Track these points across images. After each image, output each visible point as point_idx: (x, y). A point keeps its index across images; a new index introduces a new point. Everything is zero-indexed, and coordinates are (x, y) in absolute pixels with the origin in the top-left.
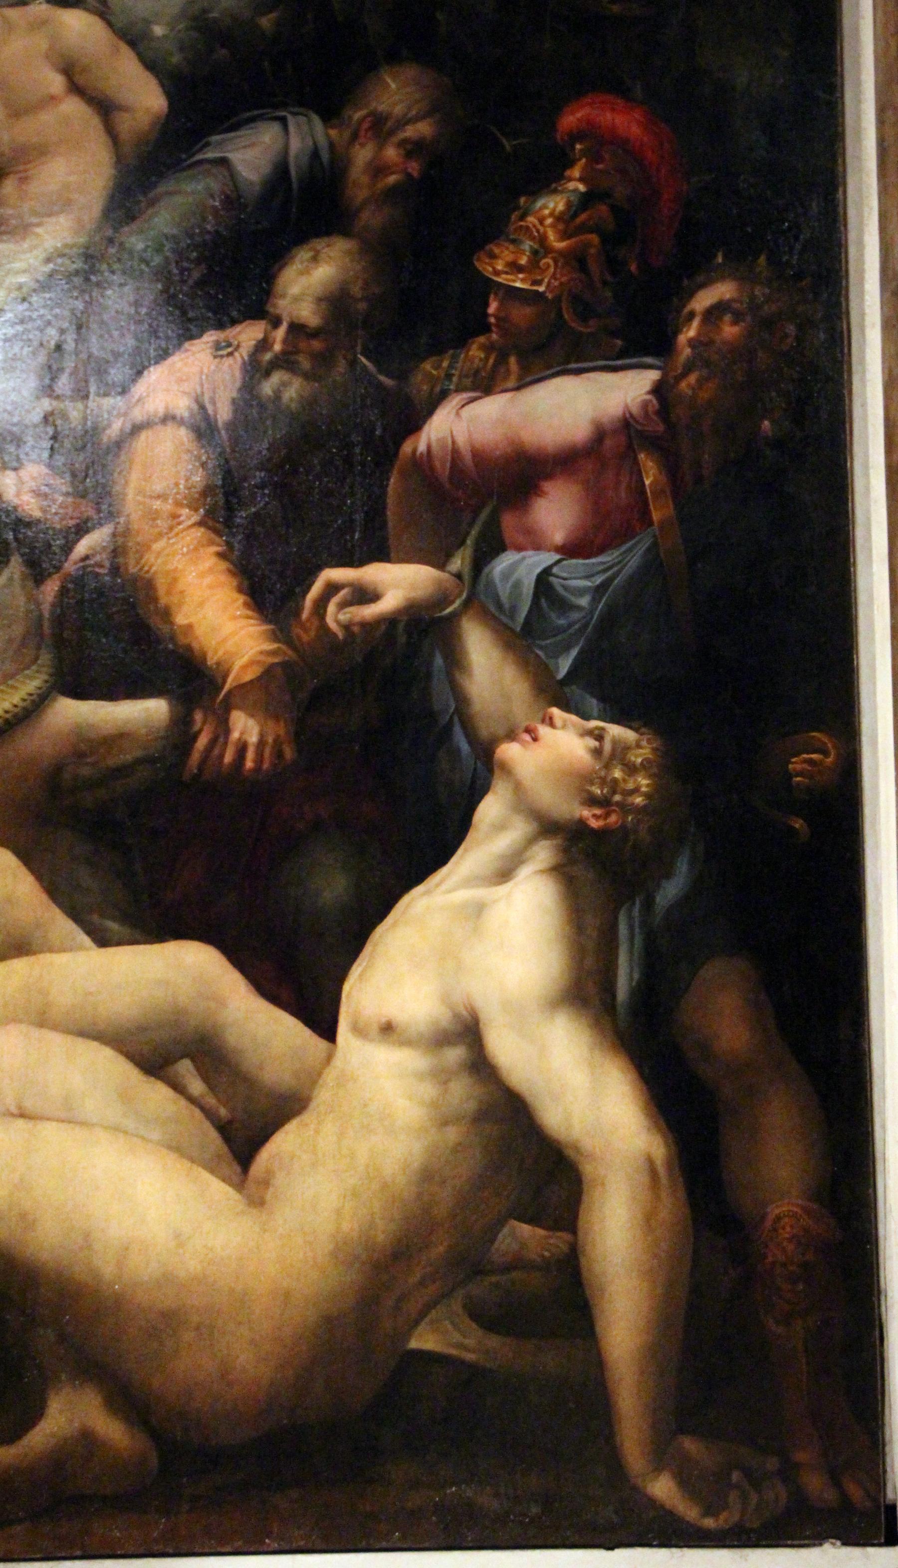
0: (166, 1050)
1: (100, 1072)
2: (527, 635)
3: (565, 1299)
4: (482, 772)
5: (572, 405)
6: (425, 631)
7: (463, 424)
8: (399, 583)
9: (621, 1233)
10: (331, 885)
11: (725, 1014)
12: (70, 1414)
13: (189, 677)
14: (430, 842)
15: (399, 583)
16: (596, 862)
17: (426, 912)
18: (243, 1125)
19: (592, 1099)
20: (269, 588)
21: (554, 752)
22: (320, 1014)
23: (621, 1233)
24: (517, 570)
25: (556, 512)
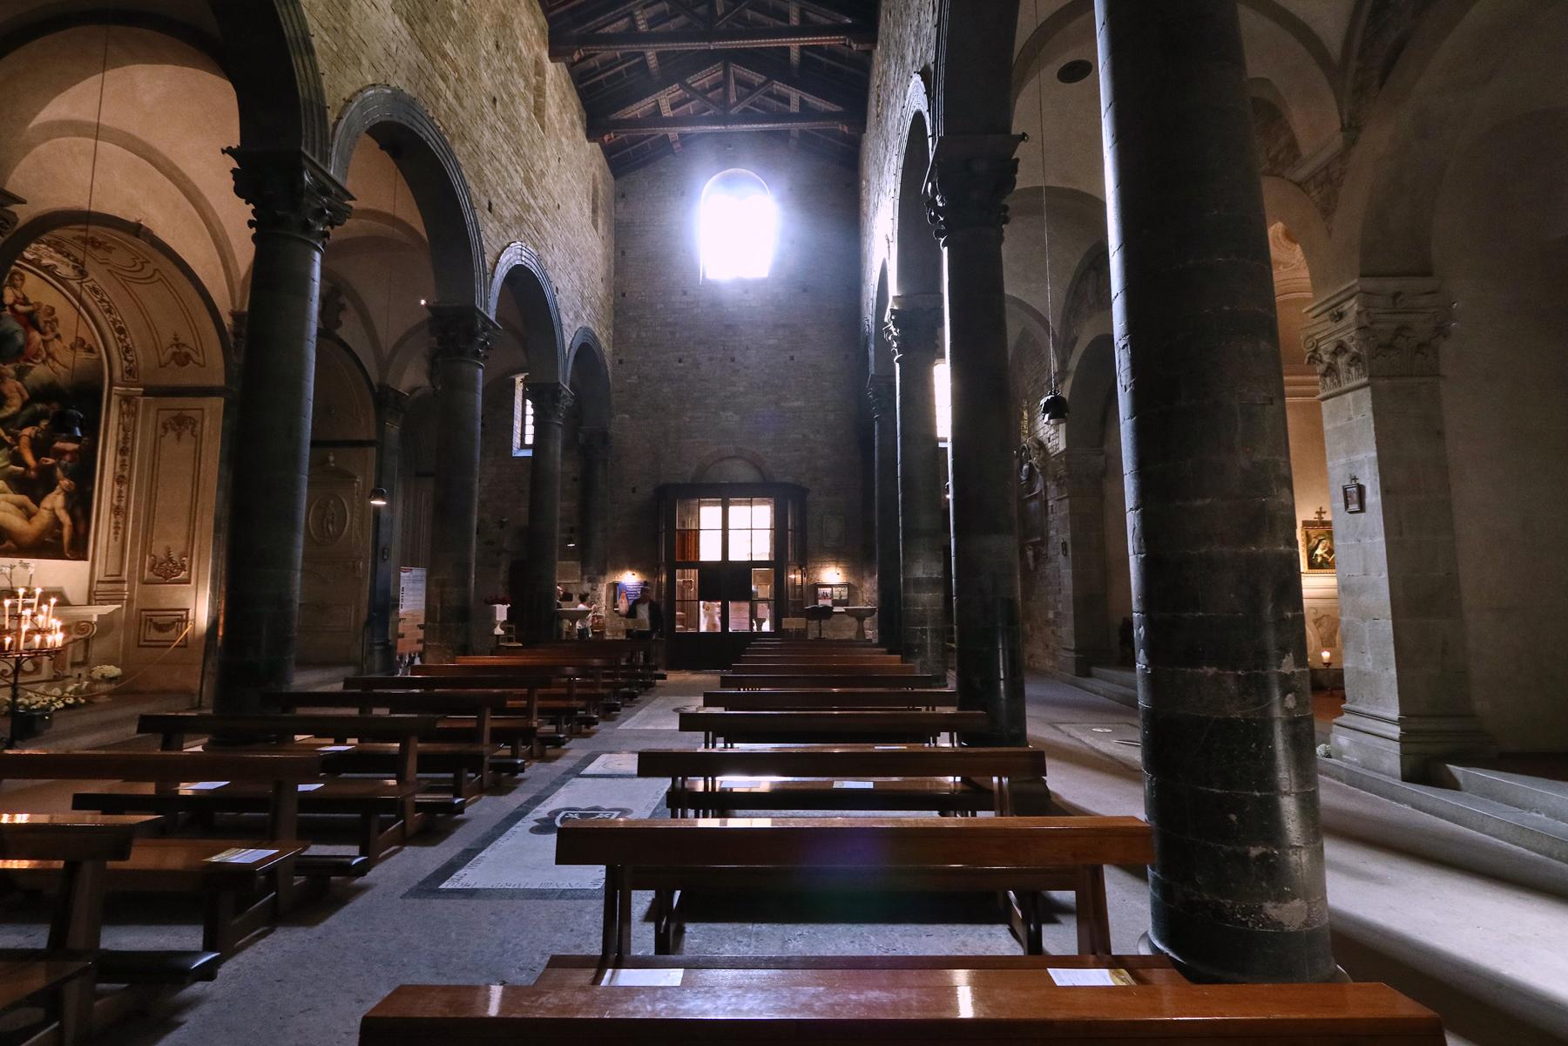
0: (21, 507)
1: (11, 507)
2: (64, 469)
3: (60, 537)
4: (57, 483)
5: (71, 446)
6: (53, 467)
7: (58, 445)
8: (51, 461)
9: (66, 532)
10: (41, 492)
11: (78, 512)
12: (8, 543)
13: (26, 466)
14: (51, 489)
15: (51, 461)
16: (68, 495)
17: (51, 496)
18: (29, 516)
19: (65, 519)
20: (37, 458)
21: (65, 482)
22: (38, 505)
23: (66, 532)
24: (63, 462)
25: (68, 457)
